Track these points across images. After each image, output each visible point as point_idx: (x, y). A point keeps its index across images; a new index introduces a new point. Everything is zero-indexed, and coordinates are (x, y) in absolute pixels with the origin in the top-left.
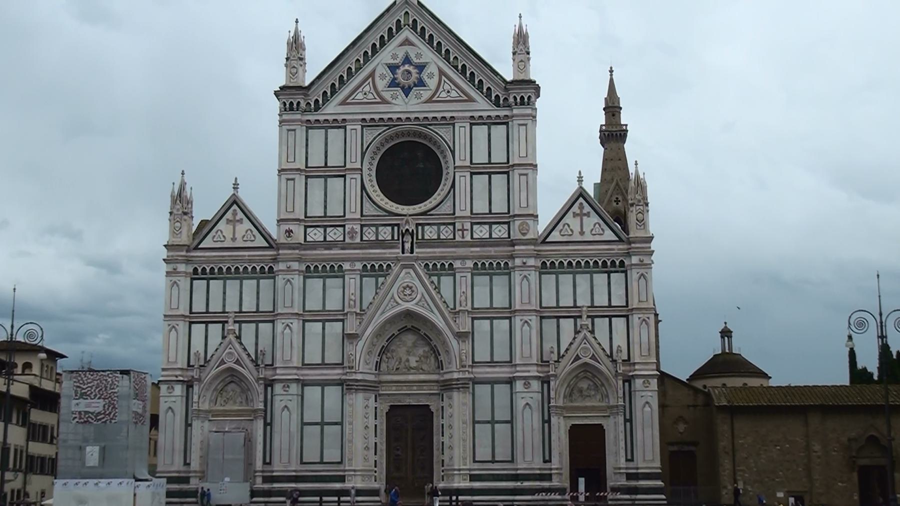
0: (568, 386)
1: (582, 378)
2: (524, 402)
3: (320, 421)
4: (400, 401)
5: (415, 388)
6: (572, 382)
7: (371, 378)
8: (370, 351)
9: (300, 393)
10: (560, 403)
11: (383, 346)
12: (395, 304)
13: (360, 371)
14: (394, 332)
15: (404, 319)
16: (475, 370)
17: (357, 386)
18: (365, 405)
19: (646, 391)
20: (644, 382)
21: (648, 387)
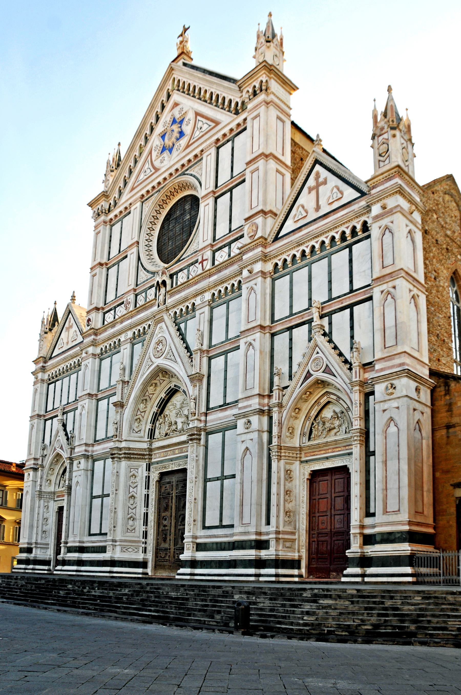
0: (307, 417)
1: (329, 403)
2: (243, 448)
3: (101, 494)
4: (165, 468)
5: (177, 451)
6: (313, 413)
7: (145, 446)
8: (139, 419)
9: (90, 467)
10: (296, 442)
11: (154, 412)
12: (151, 363)
13: (124, 438)
14: (162, 396)
15: (164, 379)
16: (209, 418)
17: (121, 454)
18: (131, 474)
19: (389, 400)
20: (387, 387)
21: (392, 394)
